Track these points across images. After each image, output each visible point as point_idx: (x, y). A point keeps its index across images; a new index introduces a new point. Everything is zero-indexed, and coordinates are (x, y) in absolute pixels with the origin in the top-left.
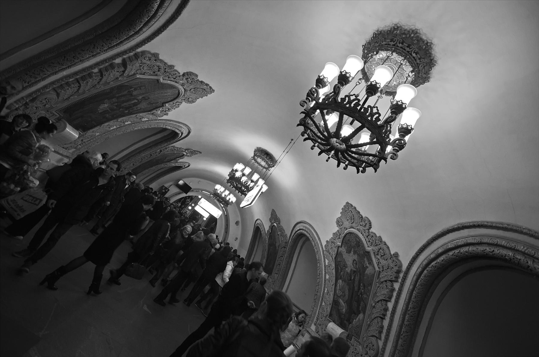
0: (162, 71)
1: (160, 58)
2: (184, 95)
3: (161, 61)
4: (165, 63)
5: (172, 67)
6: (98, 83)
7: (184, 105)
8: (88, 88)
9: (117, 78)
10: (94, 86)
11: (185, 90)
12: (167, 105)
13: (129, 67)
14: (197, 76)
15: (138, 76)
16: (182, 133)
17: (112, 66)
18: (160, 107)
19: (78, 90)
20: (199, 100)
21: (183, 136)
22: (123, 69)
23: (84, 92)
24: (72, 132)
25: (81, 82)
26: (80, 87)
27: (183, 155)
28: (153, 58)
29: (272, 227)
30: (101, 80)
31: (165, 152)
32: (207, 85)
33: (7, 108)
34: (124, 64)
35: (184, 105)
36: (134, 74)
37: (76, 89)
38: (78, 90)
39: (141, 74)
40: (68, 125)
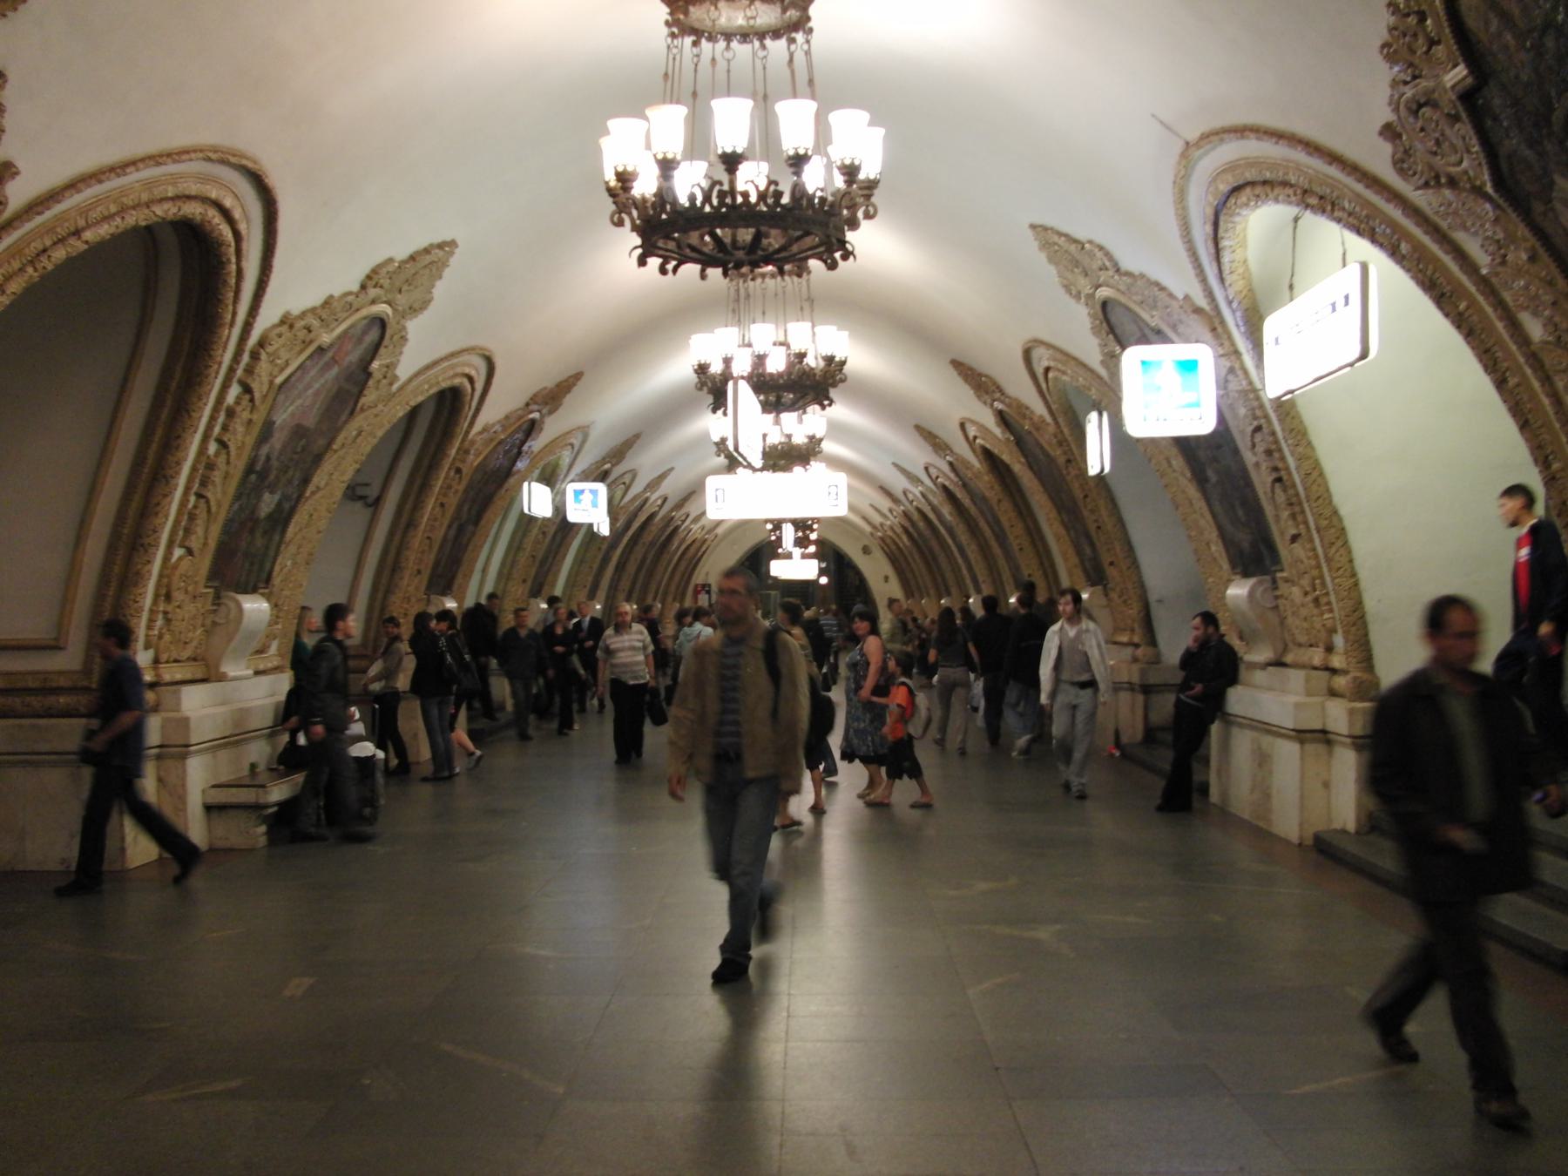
0: (316, 323)
1: (296, 312)
2: (395, 310)
3: (303, 314)
4: (313, 310)
5: (327, 303)
6: (228, 463)
7: (414, 326)
8: (219, 489)
9: (250, 421)
10: (226, 476)
11: (389, 303)
12: (375, 365)
13: (255, 386)
14: (391, 260)
15: (279, 380)
16: (471, 380)
17: (231, 413)
18: (366, 381)
19: (209, 511)
20: (440, 290)
21: (479, 386)
22: (247, 397)
23: (219, 505)
24: (255, 607)
25: (205, 493)
26: (208, 502)
27: (533, 422)
28: (284, 329)
29: (1002, 418)
30: (228, 454)
31: (473, 460)
32: (427, 251)
33: (147, 647)
35: (414, 326)
36: (271, 382)
37: (204, 515)
38: (209, 511)
39: (282, 370)
40: (240, 597)
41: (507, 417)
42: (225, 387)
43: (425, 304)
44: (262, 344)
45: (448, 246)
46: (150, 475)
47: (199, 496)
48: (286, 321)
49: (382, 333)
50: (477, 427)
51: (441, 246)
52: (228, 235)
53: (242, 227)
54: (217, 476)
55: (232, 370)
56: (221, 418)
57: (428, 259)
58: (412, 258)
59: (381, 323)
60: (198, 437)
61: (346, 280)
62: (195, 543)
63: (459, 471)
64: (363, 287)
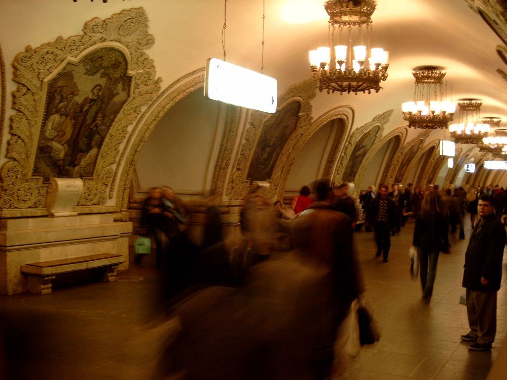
5: (366, 124)
12: (378, 135)
14: (379, 115)
15: (357, 141)
16: (402, 133)
34: (350, 143)
35: (385, 126)
41: (414, 139)
42: (345, 143)
43: (388, 122)
44: (353, 134)
45: (392, 111)
46: (331, 161)
47: (340, 163)
48: (357, 129)
49: (378, 129)
50: (405, 143)
51: (390, 111)
52: (345, 117)
53: (348, 116)
54: (344, 160)
55: (347, 140)
56: (345, 149)
57: (387, 114)
58: (384, 114)
59: (379, 127)
60: (340, 152)
61: (369, 119)
62: (339, 172)
63: (402, 153)
64: (373, 121)
